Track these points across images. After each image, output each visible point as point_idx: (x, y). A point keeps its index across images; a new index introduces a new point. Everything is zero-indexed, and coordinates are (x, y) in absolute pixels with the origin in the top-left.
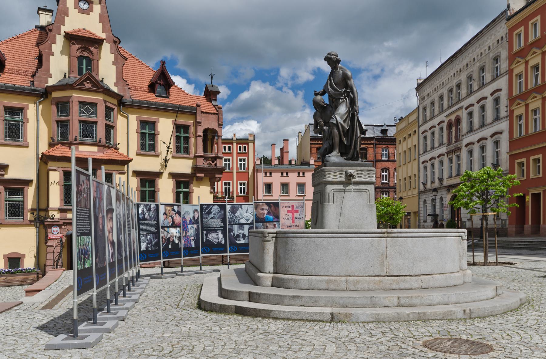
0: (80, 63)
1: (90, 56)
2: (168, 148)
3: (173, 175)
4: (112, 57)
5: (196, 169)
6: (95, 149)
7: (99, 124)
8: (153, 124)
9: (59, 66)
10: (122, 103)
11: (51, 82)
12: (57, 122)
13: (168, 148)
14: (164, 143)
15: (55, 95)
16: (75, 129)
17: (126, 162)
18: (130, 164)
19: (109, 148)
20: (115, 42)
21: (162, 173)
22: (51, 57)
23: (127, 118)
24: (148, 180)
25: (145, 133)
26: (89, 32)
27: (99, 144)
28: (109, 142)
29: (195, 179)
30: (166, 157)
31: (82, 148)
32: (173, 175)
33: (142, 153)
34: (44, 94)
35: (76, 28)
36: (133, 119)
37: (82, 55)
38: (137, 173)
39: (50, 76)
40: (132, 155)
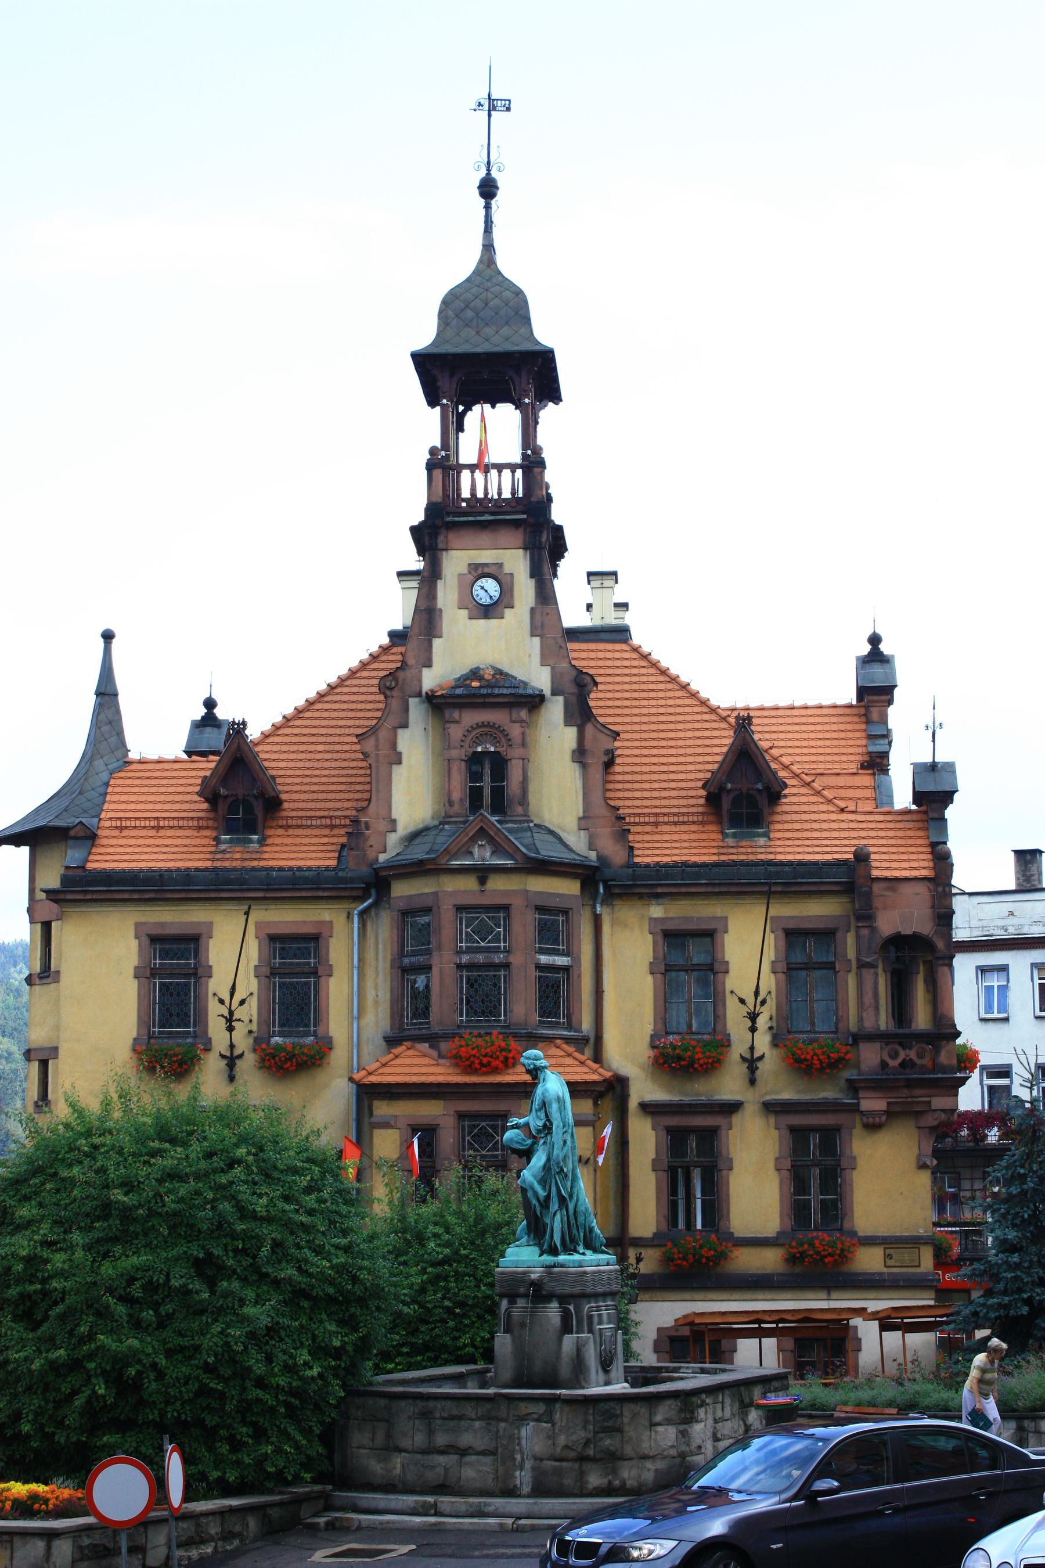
0: (475, 776)
9: (414, 793)
14: (742, 1001)
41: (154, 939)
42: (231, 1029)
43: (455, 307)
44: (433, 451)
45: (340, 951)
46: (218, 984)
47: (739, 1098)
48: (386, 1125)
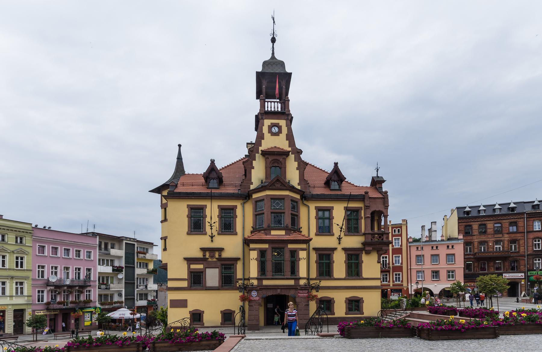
2: (341, 228)
3: (344, 249)
4: (296, 164)
5: (364, 244)
6: (283, 232)
7: (286, 213)
11: (252, 187)
12: (256, 215)
13: (341, 228)
15: (255, 196)
17: (307, 241)
18: (311, 242)
19: (295, 231)
23: (308, 207)
26: (279, 148)
27: (286, 229)
28: (294, 225)
29: (364, 252)
30: (340, 236)
31: (273, 232)
32: (344, 249)
35: (269, 147)
39: (252, 183)
40: (312, 235)
42: (211, 229)
45: (239, 212)
46: (208, 219)
48: (254, 249)
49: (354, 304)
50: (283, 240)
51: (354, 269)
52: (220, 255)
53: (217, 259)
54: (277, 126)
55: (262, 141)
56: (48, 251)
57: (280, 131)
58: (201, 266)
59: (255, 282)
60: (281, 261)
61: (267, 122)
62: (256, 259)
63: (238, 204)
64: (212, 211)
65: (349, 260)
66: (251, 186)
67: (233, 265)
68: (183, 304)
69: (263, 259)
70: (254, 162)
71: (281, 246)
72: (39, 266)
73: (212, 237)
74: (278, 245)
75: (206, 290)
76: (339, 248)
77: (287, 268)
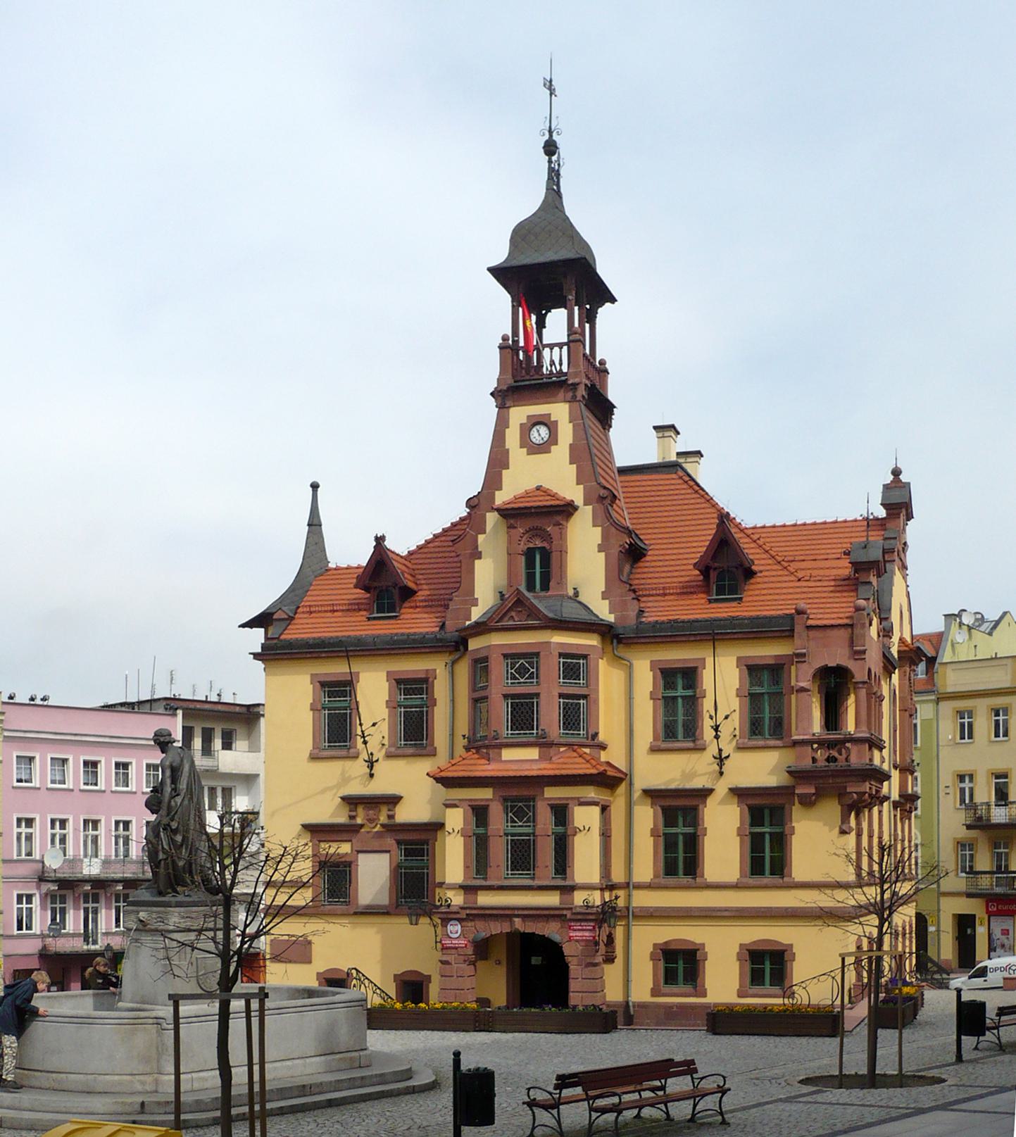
0: (530, 564)
1: (545, 545)
4: (595, 535)
5: (797, 775)
6: (533, 753)
8: (690, 675)
9: (488, 580)
10: (614, 637)
11: (476, 614)
16: (500, 712)
20: (601, 499)
21: (711, 791)
22: (477, 562)
23: (630, 667)
24: (680, 811)
25: (675, 698)
27: (544, 744)
31: (508, 754)
32: (740, 794)
33: (664, 745)
34: (456, 645)
35: (520, 490)
36: (644, 669)
37: (531, 545)
38: (652, 795)
39: (475, 603)
41: (323, 684)
43: (522, 235)
44: (505, 338)
45: (440, 689)
47: (709, 786)
49: (767, 964)
50: (526, 777)
51: (767, 855)
52: (391, 817)
53: (382, 825)
54: (546, 425)
55: (504, 472)
56: (41, 773)
57: (553, 439)
58: (345, 848)
59: (457, 899)
60: (528, 835)
61: (519, 414)
62: (463, 833)
63: (437, 665)
64: (374, 690)
65: (752, 825)
66: (473, 609)
67: (426, 842)
68: (298, 951)
69: (481, 831)
70: (481, 538)
71: (525, 792)
72: (19, 820)
73: (371, 763)
74: (519, 793)
75: (356, 913)
76: (721, 789)
77: (545, 854)
